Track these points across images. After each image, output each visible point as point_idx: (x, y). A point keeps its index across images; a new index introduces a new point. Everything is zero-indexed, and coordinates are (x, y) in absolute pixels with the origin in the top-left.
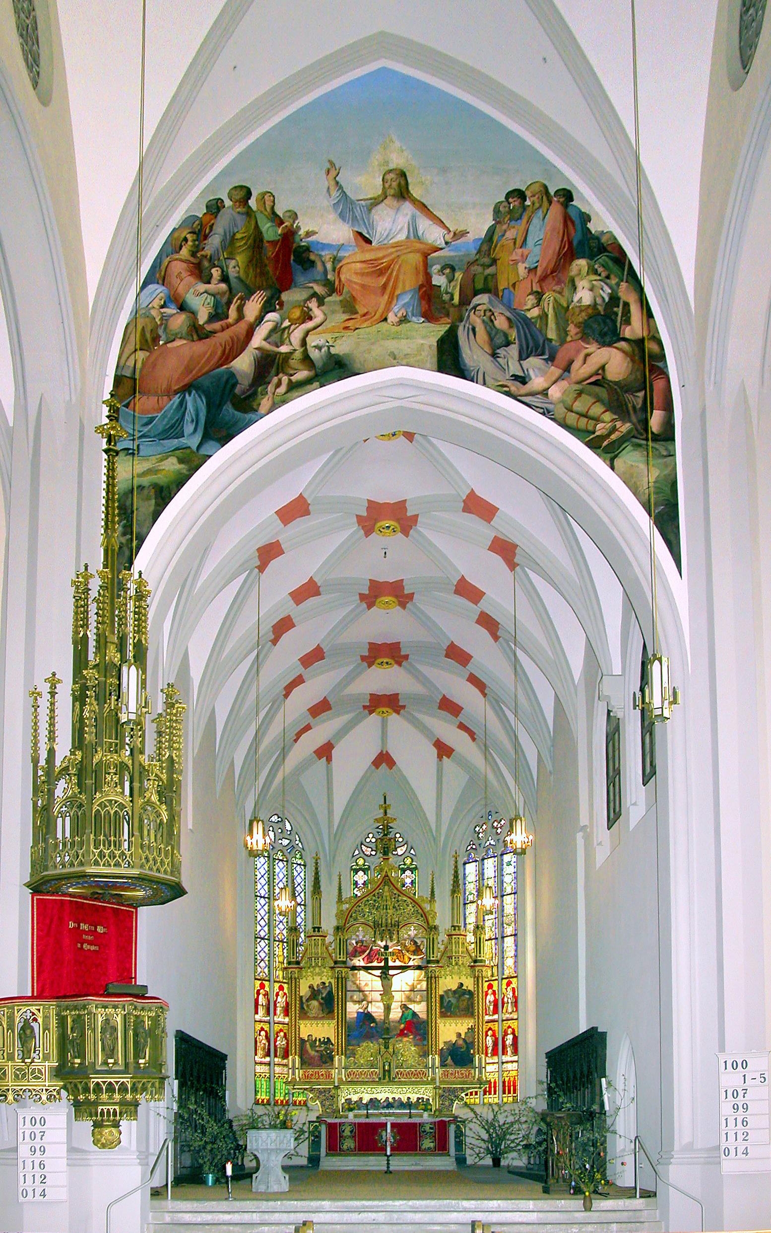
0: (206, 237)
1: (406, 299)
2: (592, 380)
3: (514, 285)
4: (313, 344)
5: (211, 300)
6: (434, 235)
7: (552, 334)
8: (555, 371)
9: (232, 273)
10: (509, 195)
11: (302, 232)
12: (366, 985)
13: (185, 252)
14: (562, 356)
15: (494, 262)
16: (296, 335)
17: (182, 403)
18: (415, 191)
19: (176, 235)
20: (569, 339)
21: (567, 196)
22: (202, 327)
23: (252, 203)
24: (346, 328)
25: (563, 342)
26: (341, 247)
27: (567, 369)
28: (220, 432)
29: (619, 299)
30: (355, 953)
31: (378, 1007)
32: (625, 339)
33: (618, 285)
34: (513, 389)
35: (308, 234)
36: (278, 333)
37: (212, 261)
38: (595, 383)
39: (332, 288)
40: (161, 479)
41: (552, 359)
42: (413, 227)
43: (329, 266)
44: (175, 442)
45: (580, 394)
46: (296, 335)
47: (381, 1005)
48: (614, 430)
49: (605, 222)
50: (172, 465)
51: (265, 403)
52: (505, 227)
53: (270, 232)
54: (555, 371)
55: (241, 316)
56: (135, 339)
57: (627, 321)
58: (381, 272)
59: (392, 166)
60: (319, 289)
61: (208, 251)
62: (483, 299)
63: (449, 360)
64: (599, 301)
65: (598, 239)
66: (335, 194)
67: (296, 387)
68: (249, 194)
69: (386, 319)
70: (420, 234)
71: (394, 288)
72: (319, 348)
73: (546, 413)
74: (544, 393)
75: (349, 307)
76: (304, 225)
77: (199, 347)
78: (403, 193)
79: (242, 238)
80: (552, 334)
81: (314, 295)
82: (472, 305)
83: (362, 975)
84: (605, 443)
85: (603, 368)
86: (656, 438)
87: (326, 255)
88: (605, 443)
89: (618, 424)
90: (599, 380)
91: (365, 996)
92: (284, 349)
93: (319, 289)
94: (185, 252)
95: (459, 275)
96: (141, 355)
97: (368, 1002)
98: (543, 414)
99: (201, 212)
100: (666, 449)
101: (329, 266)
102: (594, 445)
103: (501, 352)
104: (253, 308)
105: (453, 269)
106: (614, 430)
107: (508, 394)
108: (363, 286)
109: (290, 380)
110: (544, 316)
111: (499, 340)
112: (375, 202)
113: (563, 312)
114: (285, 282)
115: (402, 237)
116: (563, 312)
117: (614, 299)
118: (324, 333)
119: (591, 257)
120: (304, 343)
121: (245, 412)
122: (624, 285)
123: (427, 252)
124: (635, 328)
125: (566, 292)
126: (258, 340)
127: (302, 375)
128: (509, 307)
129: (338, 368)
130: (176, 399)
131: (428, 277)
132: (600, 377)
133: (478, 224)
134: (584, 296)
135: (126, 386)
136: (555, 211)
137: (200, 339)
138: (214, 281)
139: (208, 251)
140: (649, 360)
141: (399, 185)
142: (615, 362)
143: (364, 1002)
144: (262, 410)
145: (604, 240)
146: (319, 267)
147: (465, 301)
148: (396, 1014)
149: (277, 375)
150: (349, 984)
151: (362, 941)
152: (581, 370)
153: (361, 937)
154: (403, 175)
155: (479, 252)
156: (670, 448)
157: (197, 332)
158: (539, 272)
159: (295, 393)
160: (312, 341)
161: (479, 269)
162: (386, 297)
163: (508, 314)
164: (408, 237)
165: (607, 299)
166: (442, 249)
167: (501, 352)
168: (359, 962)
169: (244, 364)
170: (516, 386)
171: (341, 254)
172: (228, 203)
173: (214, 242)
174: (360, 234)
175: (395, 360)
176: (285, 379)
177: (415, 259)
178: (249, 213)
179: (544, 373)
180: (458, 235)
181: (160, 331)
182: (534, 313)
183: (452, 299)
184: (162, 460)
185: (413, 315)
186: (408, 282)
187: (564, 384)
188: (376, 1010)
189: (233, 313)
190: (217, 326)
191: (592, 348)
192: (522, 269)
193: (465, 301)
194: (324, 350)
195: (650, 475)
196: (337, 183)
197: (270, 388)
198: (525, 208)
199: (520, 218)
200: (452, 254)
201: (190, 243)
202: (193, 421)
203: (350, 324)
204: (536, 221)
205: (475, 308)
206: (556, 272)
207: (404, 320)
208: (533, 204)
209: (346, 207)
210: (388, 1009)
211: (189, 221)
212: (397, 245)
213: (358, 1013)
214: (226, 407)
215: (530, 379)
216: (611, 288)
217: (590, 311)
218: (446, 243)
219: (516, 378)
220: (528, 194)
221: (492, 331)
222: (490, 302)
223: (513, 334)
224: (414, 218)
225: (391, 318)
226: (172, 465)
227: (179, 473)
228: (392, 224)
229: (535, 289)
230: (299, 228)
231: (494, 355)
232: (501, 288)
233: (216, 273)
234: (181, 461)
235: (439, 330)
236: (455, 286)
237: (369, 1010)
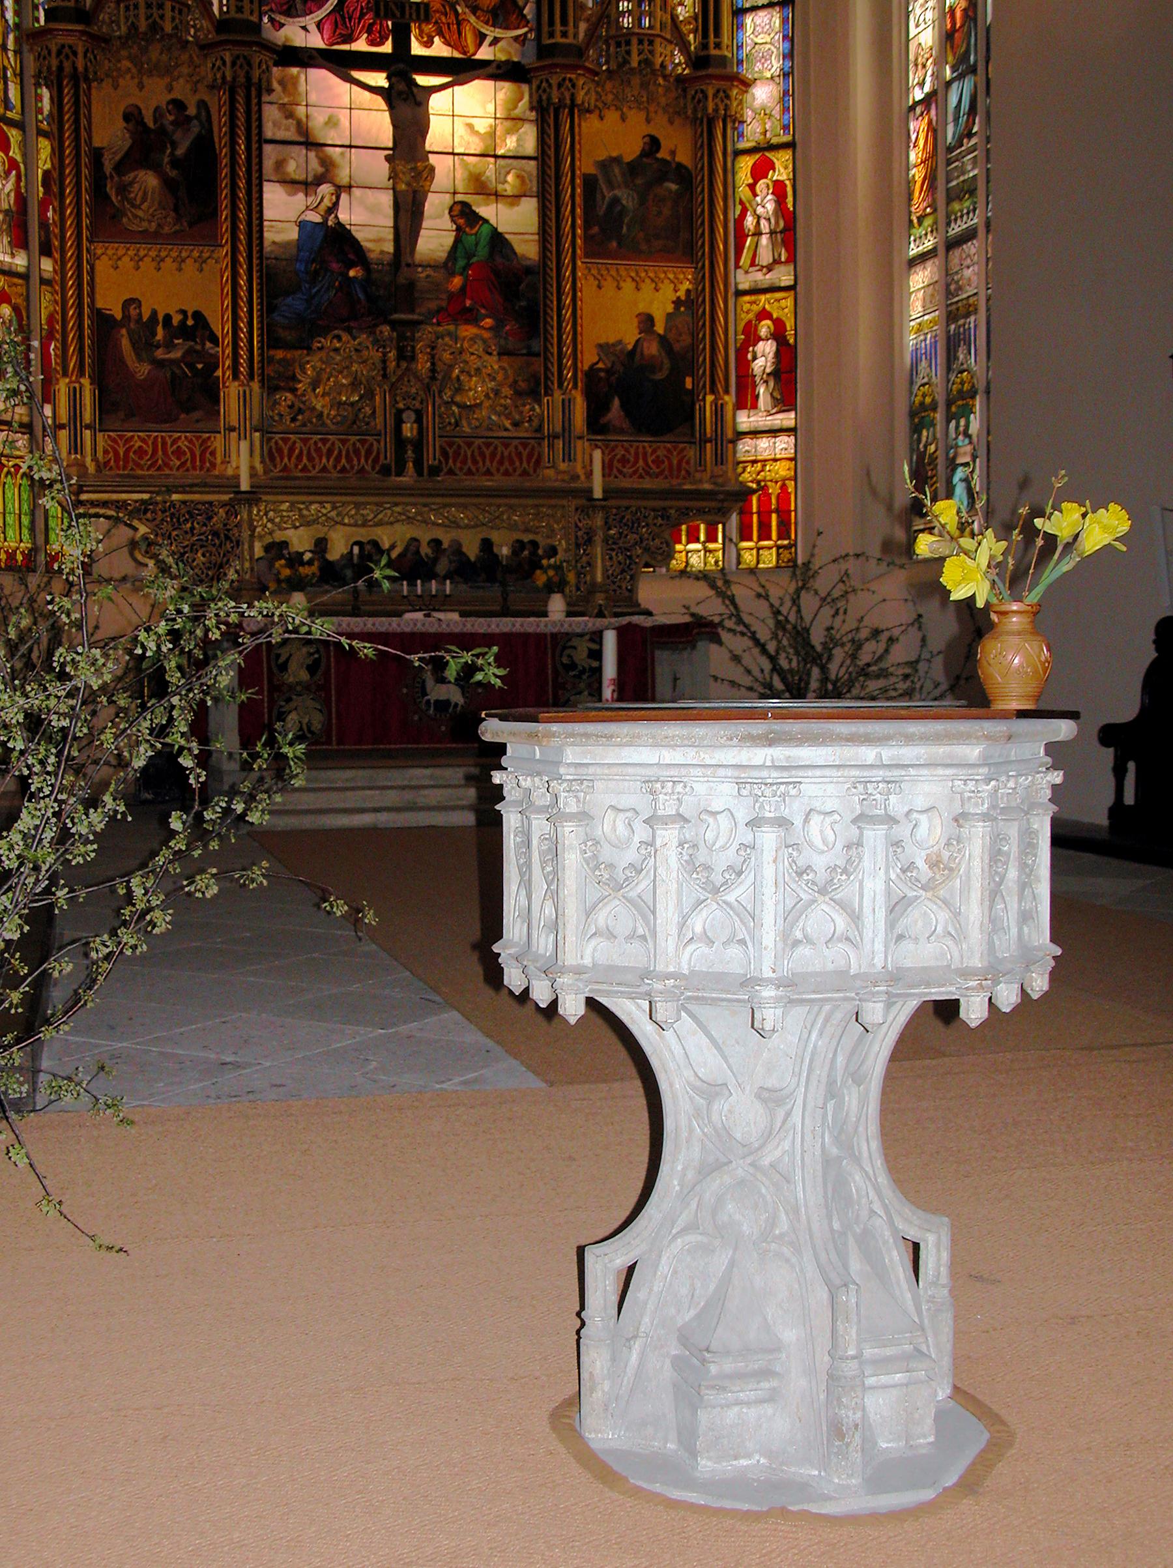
31: (373, 209)
47: (386, 200)
91: (328, 165)
97: (339, 189)
143: (325, 189)
148: (435, 237)
150: (271, 113)
188: (368, 217)
213: (302, 225)
237: (343, 216)
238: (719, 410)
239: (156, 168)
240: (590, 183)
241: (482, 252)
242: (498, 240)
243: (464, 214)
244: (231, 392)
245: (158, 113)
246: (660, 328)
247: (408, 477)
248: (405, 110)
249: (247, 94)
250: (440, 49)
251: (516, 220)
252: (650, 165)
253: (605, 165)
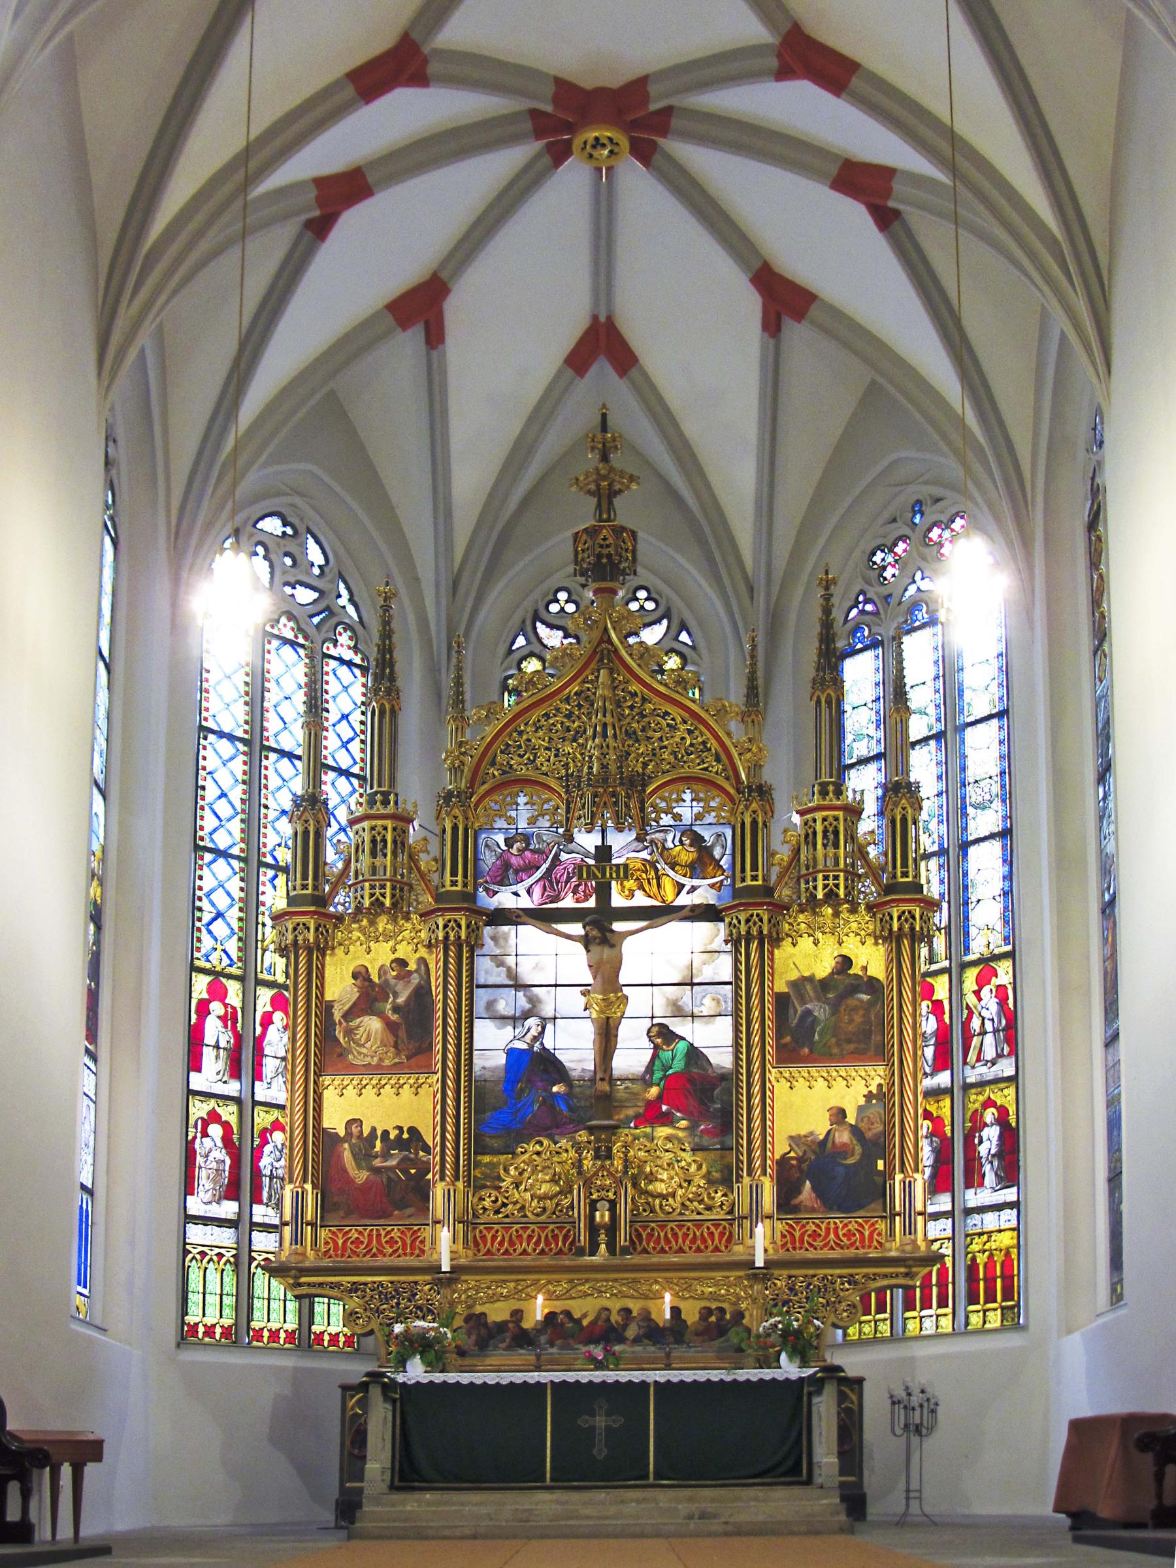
30: (504, 875)
91: (534, 1001)
143: (532, 1022)
148: (632, 1055)
151: (527, 838)
188: (573, 1045)
213: (511, 1053)
237: (548, 1043)
239: (381, 1015)
245: (382, 971)
250: (641, 900)
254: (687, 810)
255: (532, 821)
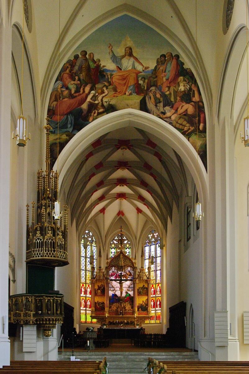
0: (74, 67)
1: (131, 87)
2: (183, 114)
3: (162, 84)
4: (105, 101)
5: (75, 86)
6: (139, 68)
7: (172, 99)
8: (173, 111)
9: (81, 78)
10: (161, 56)
11: (102, 66)
12: (115, 285)
13: (68, 71)
14: (175, 106)
15: (156, 77)
16: (100, 98)
17: (67, 118)
18: (134, 54)
19: (65, 65)
20: (177, 101)
21: (177, 57)
22: (73, 94)
23: (87, 56)
24: (114, 96)
25: (176, 102)
26: (113, 71)
27: (177, 110)
28: (78, 127)
29: (192, 89)
30: (112, 275)
31: (119, 293)
32: (193, 102)
33: (191, 85)
34: (161, 116)
35: (104, 66)
36: (95, 97)
37: (76, 74)
38: (185, 115)
39: (110, 84)
40: (62, 141)
41: (172, 107)
42: (133, 65)
43: (109, 77)
44: (65, 130)
45: (180, 118)
46: (100, 98)
47: (120, 292)
48: (189, 129)
49: (188, 65)
50: (64, 137)
51: (91, 119)
52: (160, 66)
53: (92, 65)
54: (173, 111)
55: (84, 92)
56: (53, 98)
57: (194, 96)
58: (124, 79)
59: (127, 46)
60: (106, 84)
61: (74, 71)
62: (153, 88)
63: (143, 107)
64: (186, 90)
65: (186, 70)
66: (111, 54)
67: (100, 114)
68: (86, 53)
69: (125, 94)
70: (135, 67)
71: (128, 83)
72: (106, 102)
73: (170, 123)
74: (170, 117)
75: (115, 90)
76: (102, 64)
77: (72, 101)
78: (131, 55)
79: (84, 67)
80: (172, 99)
81: (105, 86)
82: (150, 90)
83: (114, 283)
84: (187, 133)
85: (187, 110)
86: (201, 132)
87: (109, 73)
88: (187, 133)
89: (191, 127)
90: (185, 114)
91: (115, 289)
92: (96, 102)
93: (106, 84)
94: (68, 71)
95: (146, 81)
96: (55, 103)
97: (116, 291)
98: (170, 124)
99: (72, 59)
100: (204, 135)
101: (109, 77)
102: (184, 133)
103: (158, 105)
104: (87, 89)
105: (145, 79)
106: (189, 129)
107: (160, 118)
108: (119, 83)
109: (98, 112)
110: (170, 94)
111: (158, 101)
112: (123, 57)
113: (176, 92)
114: (98, 82)
115: (130, 68)
116: (176, 92)
117: (190, 89)
118: (107, 98)
119: (184, 76)
120: (102, 100)
121: (86, 121)
122: (193, 85)
123: (138, 73)
124: (196, 98)
125: (177, 87)
126: (89, 99)
127: (101, 110)
128: (160, 90)
129: (111, 108)
130: (65, 117)
131: (138, 81)
132: (186, 113)
133: (152, 65)
134: (182, 88)
135: (51, 112)
136: (174, 61)
137: (72, 98)
138: (76, 80)
139: (74, 71)
140: (200, 108)
141: (130, 52)
142: (190, 108)
143: (114, 291)
144: (90, 121)
145: (188, 71)
146: (107, 77)
147: (148, 89)
148: (124, 294)
149: (94, 110)
150: (110, 285)
151: (114, 272)
152: (180, 111)
153: (113, 270)
154: (131, 49)
155: (152, 73)
156: (205, 135)
157: (71, 96)
158: (169, 80)
159: (99, 116)
160: (105, 100)
161: (152, 79)
162: (126, 87)
163: (160, 93)
164: (132, 68)
165: (188, 89)
166: (141, 72)
167: (158, 105)
168: (113, 278)
169: (85, 106)
170: (162, 115)
171: (113, 73)
172: (80, 56)
173: (76, 68)
174: (118, 67)
175: (128, 106)
176: (97, 111)
177: (134, 75)
178: (86, 60)
179: (170, 111)
180: (146, 68)
181: (61, 95)
182: (168, 93)
183: (144, 88)
184: (61, 135)
185: (133, 92)
186: (132, 82)
187: (175, 115)
188: (118, 293)
189: (82, 91)
190: (77, 94)
191: (184, 104)
192: (164, 79)
193: (148, 89)
194: (108, 103)
195: (199, 143)
196: (112, 51)
197: (92, 114)
198: (165, 60)
199: (164, 63)
200: (145, 74)
201: (69, 68)
202: (70, 124)
203: (115, 95)
204: (169, 65)
205: (151, 91)
206: (174, 81)
207: (131, 94)
208: (168, 59)
209: (115, 59)
210: (121, 293)
211: (69, 61)
212: (129, 71)
213: (113, 294)
214: (80, 120)
215: (166, 113)
216: (189, 86)
217: (183, 92)
218: (143, 71)
219: (162, 113)
220: (167, 56)
221: (155, 98)
222: (155, 89)
223: (162, 99)
224: (134, 62)
225: (127, 93)
226: (64, 137)
227: (66, 139)
228: (127, 64)
229: (168, 86)
230: (101, 65)
231: (156, 106)
232: (158, 85)
233: (77, 78)
234: (67, 136)
235: (141, 97)
236: (145, 84)
237: (116, 293)
238: (149, 309)
239: (100, 290)
240: (138, 289)
241: (128, 296)
242: (130, 295)
243: (127, 293)
244: (106, 309)
245: (100, 285)
246: (144, 302)
247: (121, 316)
248: (121, 285)
249: (108, 284)
250: (125, 279)
251: (131, 293)
252: (143, 288)
253: (139, 288)
254: (129, 269)
255: (114, 270)
